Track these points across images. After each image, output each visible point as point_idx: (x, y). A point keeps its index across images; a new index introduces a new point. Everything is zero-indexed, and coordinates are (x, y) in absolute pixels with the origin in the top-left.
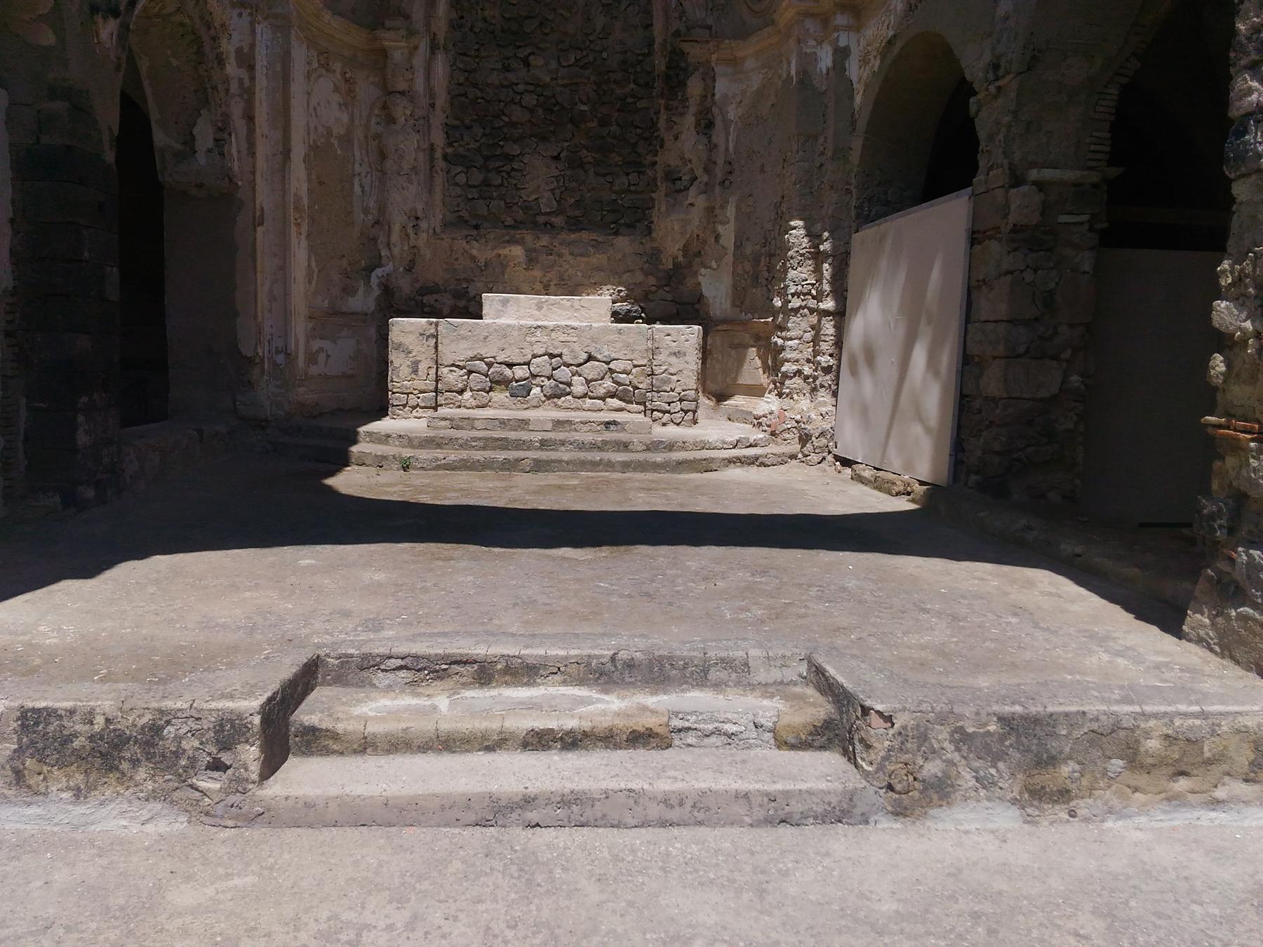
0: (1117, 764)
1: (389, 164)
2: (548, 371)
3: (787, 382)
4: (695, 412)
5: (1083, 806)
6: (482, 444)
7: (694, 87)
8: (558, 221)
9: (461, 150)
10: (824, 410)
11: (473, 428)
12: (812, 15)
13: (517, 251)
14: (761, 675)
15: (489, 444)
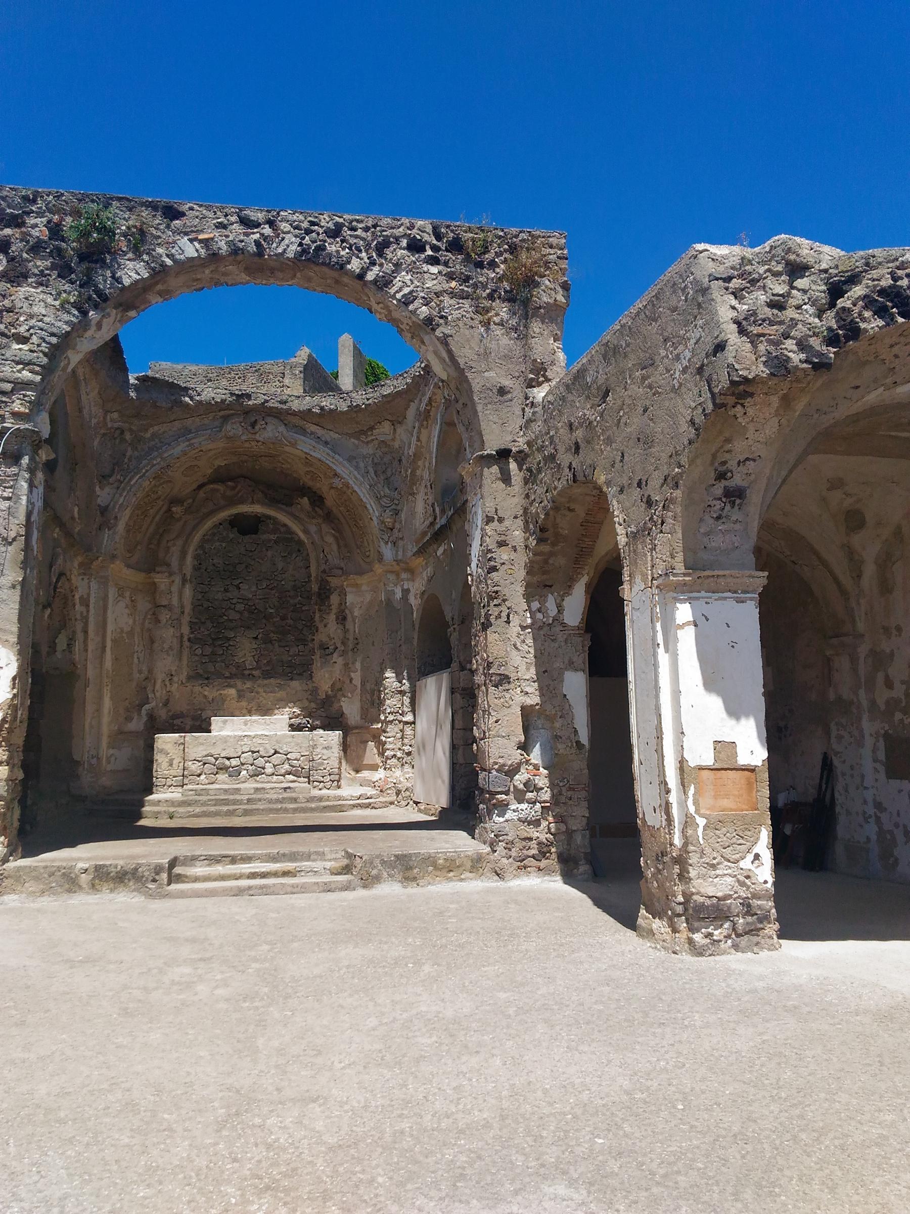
0: (431, 868)
1: (156, 645)
2: (251, 761)
3: (388, 761)
4: (338, 781)
5: (421, 882)
6: (213, 802)
7: (334, 599)
8: (256, 673)
9: (199, 636)
10: (407, 776)
11: (208, 794)
12: (392, 572)
13: (232, 691)
14: (329, 857)
15: (218, 802)
